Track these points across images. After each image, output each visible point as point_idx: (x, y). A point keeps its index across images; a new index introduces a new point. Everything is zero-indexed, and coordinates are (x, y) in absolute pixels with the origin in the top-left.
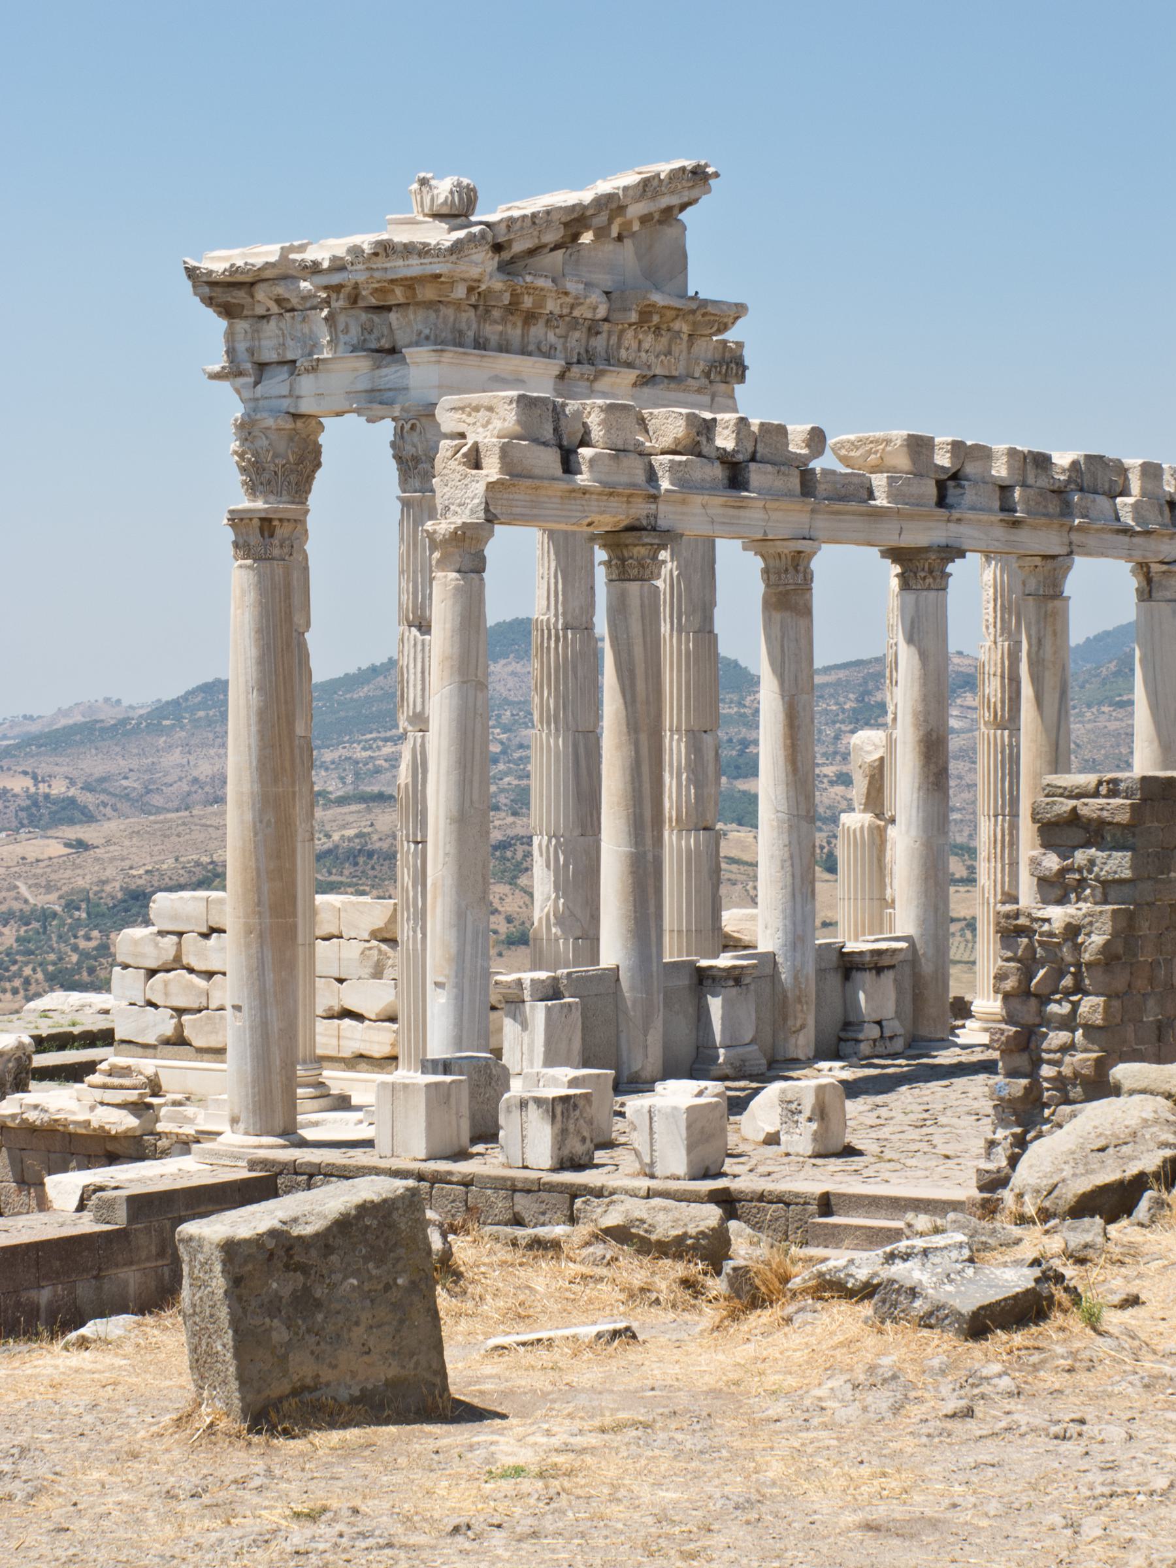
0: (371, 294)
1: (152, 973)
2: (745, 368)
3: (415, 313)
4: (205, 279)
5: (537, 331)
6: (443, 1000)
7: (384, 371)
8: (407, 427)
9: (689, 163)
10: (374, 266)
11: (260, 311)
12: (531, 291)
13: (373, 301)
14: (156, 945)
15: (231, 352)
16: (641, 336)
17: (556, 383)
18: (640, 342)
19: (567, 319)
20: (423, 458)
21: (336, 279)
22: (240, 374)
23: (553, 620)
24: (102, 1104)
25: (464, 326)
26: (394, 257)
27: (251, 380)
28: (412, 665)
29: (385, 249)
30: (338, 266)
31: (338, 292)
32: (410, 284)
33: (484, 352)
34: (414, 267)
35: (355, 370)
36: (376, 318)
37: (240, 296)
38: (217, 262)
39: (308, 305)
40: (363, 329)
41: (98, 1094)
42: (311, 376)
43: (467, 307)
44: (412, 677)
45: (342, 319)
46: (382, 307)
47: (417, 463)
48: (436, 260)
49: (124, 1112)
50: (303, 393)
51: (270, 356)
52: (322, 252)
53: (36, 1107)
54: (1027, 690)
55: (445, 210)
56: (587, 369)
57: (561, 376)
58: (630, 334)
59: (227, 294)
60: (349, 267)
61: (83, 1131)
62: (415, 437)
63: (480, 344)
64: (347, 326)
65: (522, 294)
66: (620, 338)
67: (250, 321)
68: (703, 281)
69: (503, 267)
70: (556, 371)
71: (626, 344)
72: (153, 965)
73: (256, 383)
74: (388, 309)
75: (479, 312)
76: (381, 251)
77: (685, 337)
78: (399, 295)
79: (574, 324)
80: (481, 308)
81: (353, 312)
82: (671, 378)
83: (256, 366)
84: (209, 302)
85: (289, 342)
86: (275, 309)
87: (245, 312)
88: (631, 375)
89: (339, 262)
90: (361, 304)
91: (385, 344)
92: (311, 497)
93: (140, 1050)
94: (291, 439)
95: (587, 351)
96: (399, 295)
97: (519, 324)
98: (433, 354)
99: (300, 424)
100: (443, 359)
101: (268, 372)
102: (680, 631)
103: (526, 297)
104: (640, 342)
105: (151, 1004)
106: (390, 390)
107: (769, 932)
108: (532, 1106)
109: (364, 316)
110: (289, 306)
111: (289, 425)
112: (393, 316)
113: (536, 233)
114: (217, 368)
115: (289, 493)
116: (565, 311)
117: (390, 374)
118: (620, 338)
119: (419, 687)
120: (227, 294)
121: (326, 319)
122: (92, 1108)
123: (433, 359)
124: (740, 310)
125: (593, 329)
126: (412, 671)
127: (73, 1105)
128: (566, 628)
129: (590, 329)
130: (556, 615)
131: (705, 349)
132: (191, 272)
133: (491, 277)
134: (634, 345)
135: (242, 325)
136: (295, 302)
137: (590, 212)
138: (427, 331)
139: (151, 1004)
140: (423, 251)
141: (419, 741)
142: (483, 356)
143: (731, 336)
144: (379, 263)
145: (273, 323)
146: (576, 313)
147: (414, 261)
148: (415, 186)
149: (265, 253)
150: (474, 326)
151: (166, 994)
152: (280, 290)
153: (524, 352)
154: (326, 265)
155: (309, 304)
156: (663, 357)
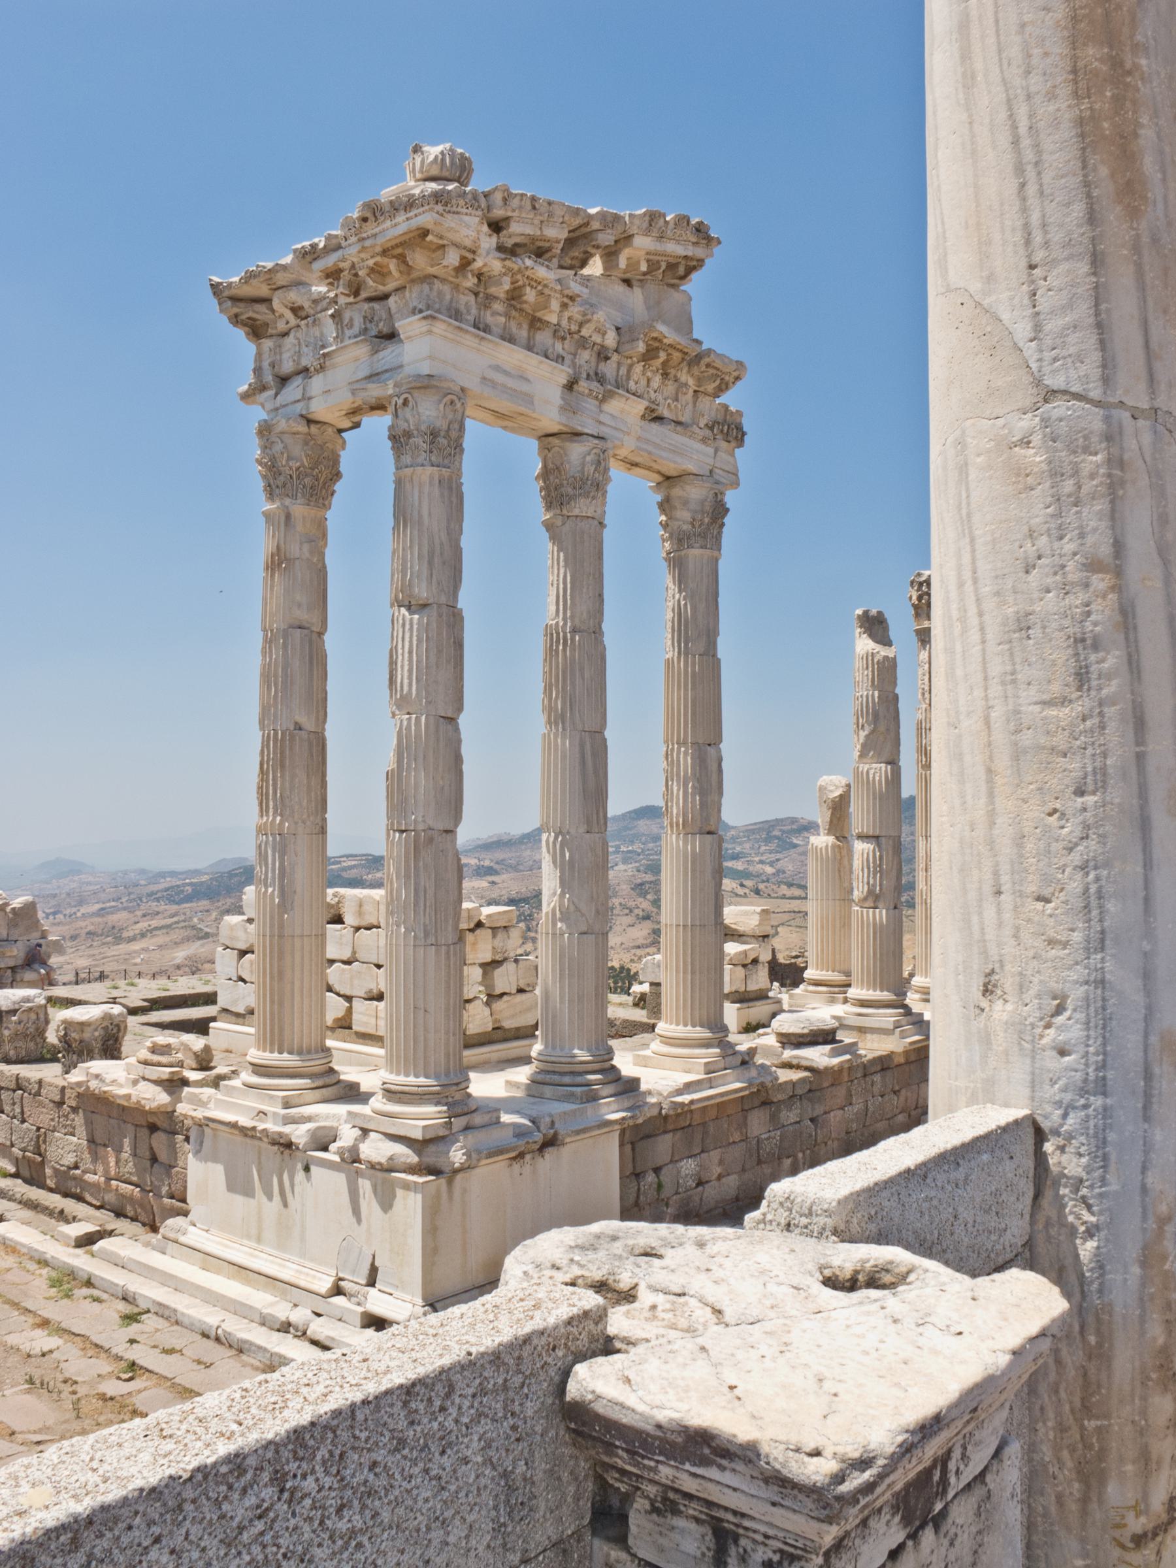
0: (368, 275)
2: (744, 434)
3: (411, 291)
4: (226, 293)
5: (543, 338)
7: (381, 354)
8: (400, 402)
10: (365, 235)
11: (281, 326)
12: (533, 283)
14: (246, 930)
15: (258, 371)
16: (649, 374)
17: (563, 393)
18: (649, 380)
19: (576, 336)
20: (415, 432)
23: (561, 624)
24: (144, 1079)
25: (462, 308)
26: (382, 218)
27: (272, 392)
28: (400, 646)
31: (338, 279)
33: (482, 334)
35: (357, 359)
36: (376, 305)
39: (319, 308)
40: (365, 317)
43: (467, 292)
44: (400, 658)
45: (347, 315)
46: (376, 283)
47: (409, 438)
48: (421, 210)
49: (159, 1089)
50: (313, 394)
51: (287, 367)
53: (97, 1076)
55: (435, 171)
56: (595, 385)
57: (570, 386)
58: (638, 368)
59: (249, 309)
60: (344, 244)
63: (481, 327)
64: (351, 320)
65: (524, 286)
66: (629, 371)
67: (275, 339)
69: (500, 248)
70: (563, 380)
71: (635, 377)
72: (243, 947)
73: (276, 395)
74: (385, 297)
75: (479, 300)
76: (368, 215)
77: (691, 392)
79: (583, 343)
80: (481, 295)
82: (678, 423)
83: (278, 380)
84: (236, 320)
86: (293, 321)
87: (270, 331)
88: (640, 406)
89: (334, 241)
90: (364, 295)
93: (234, 1018)
94: (306, 443)
95: (596, 374)
97: (525, 326)
98: (424, 323)
99: (314, 429)
100: (435, 330)
102: (686, 655)
103: (528, 289)
104: (649, 380)
106: (386, 371)
107: (1001, 1011)
109: (366, 306)
110: (303, 314)
111: (302, 428)
113: (536, 222)
115: (304, 496)
116: (574, 328)
117: (389, 355)
118: (629, 371)
119: (406, 668)
121: (332, 316)
122: (135, 1083)
123: (424, 329)
125: (603, 355)
126: (400, 651)
128: (574, 631)
129: (599, 354)
130: (565, 619)
131: (709, 408)
132: (215, 287)
133: (488, 253)
134: (643, 382)
135: (268, 344)
137: (595, 225)
141: (405, 723)
142: (483, 338)
143: (731, 399)
144: (371, 229)
145: (292, 335)
146: (585, 332)
150: (474, 311)
152: (293, 296)
153: (530, 348)
156: (669, 401)
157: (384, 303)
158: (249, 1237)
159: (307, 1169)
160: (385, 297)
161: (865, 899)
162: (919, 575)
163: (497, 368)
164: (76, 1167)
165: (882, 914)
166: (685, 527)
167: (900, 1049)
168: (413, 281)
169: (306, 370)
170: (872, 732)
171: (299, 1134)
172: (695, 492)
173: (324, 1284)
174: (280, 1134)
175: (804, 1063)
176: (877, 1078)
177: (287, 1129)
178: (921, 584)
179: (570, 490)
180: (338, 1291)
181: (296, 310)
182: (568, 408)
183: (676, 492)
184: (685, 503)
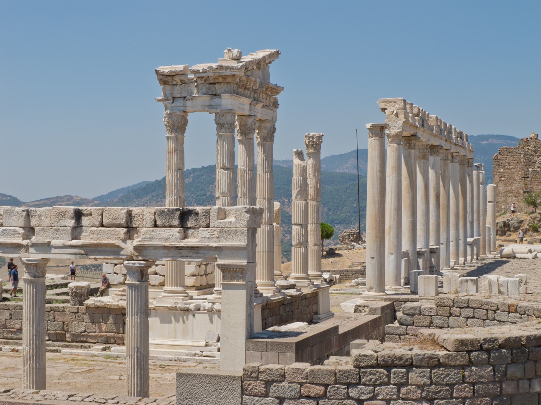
1: (116, 265)
6: (393, 258)
7: (214, 100)
8: (221, 115)
9: (273, 51)
11: (174, 83)
13: (212, 81)
15: (165, 94)
21: (203, 75)
22: (168, 100)
24: (121, 300)
27: (171, 102)
29: (220, 67)
30: (205, 71)
32: (224, 77)
34: (229, 72)
36: (211, 86)
37: (169, 79)
38: (166, 69)
41: (120, 297)
42: (191, 101)
45: (200, 86)
51: (177, 94)
52: (200, 67)
53: (99, 301)
54: (441, 184)
55: (236, 58)
57: (250, 104)
61: (116, 307)
62: (223, 118)
68: (273, 80)
73: (172, 103)
74: (215, 84)
78: (221, 80)
81: (205, 84)
85: (184, 92)
86: (179, 82)
88: (261, 105)
90: (207, 82)
91: (214, 93)
92: (185, 134)
94: (182, 118)
96: (221, 80)
101: (175, 100)
105: (115, 273)
108: (469, 281)
109: (207, 85)
112: (216, 86)
114: (160, 98)
117: (216, 101)
120: (166, 79)
121: (196, 86)
122: (118, 301)
124: (283, 89)
127: (111, 300)
128: (249, 171)
132: (157, 72)
135: (168, 87)
136: (186, 81)
138: (227, 90)
139: (115, 273)
140: (232, 68)
145: (178, 86)
147: (229, 71)
148: (226, 51)
149: (179, 67)
151: (121, 270)
152: (183, 78)
154: (201, 71)
155: (191, 81)
157: (214, 85)
158: (171, 338)
159: (194, 316)
160: (215, 84)
161: (297, 244)
162: (309, 134)
163: (240, 103)
164: (85, 331)
165: (303, 249)
166: (266, 135)
167: (310, 292)
168: (225, 83)
169: (185, 97)
170: (300, 190)
171: (192, 307)
172: (268, 125)
173: (203, 344)
174: (185, 307)
175: (289, 294)
176: (304, 301)
177: (187, 306)
178: (310, 137)
179: (248, 131)
180: (206, 345)
181: (181, 81)
182: (250, 110)
183: (263, 124)
184: (266, 128)
